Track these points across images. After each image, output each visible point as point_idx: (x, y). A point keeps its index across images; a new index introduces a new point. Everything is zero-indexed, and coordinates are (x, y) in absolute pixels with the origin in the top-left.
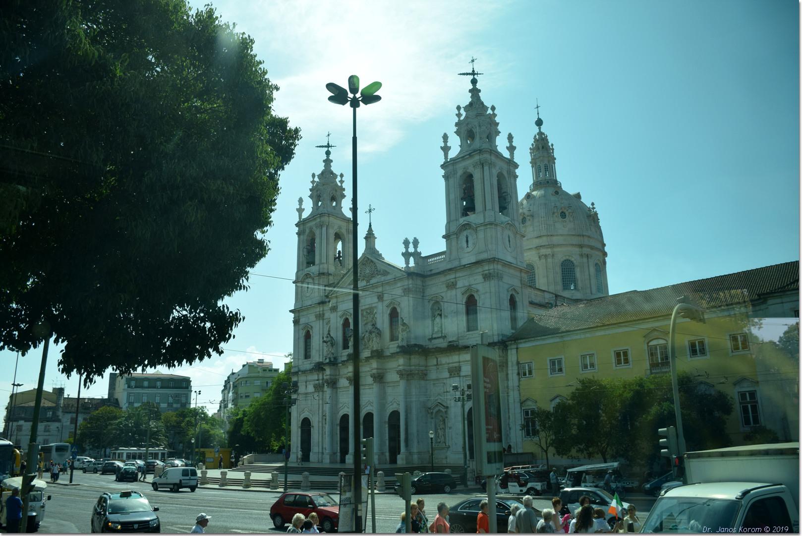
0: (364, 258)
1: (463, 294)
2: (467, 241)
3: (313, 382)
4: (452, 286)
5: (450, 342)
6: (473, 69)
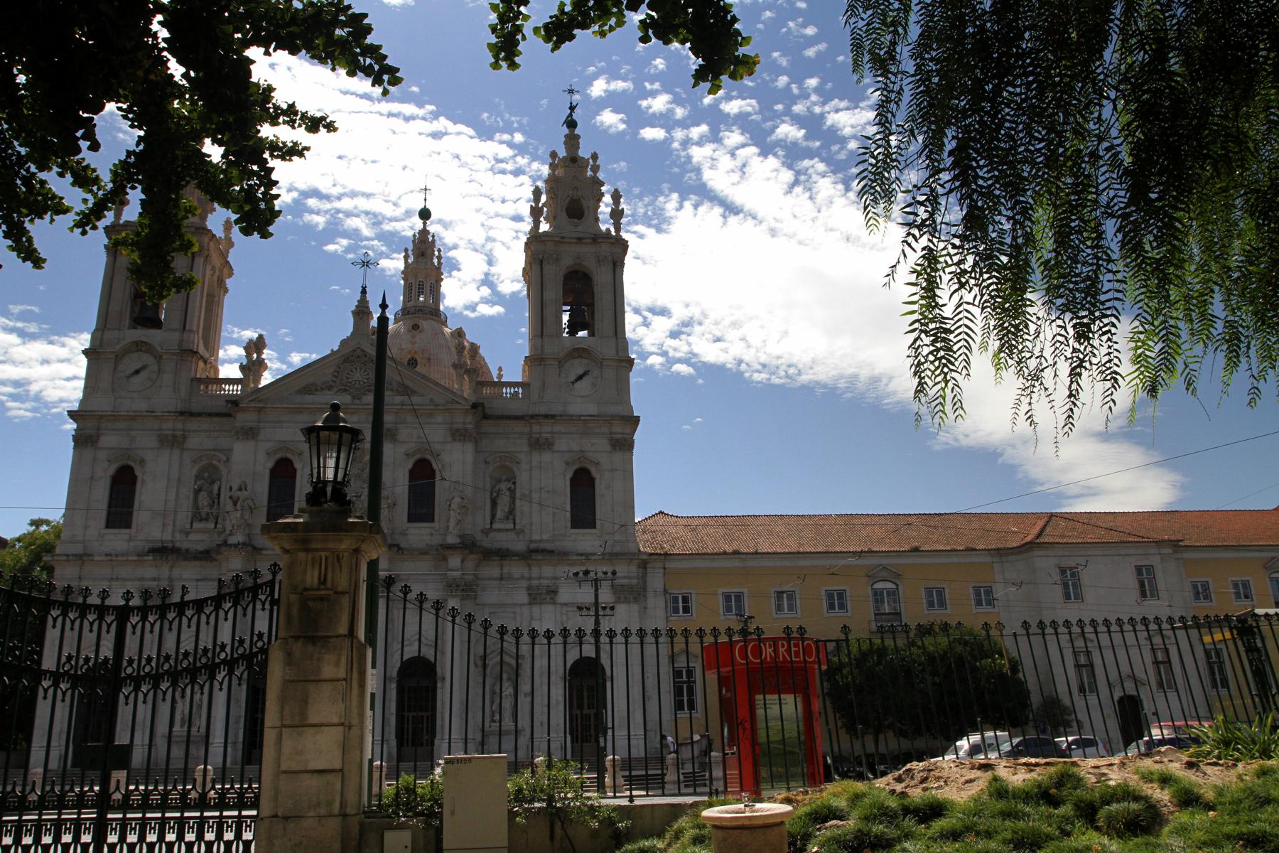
0: (354, 351)
1: (567, 464)
3: (139, 583)
4: (539, 444)
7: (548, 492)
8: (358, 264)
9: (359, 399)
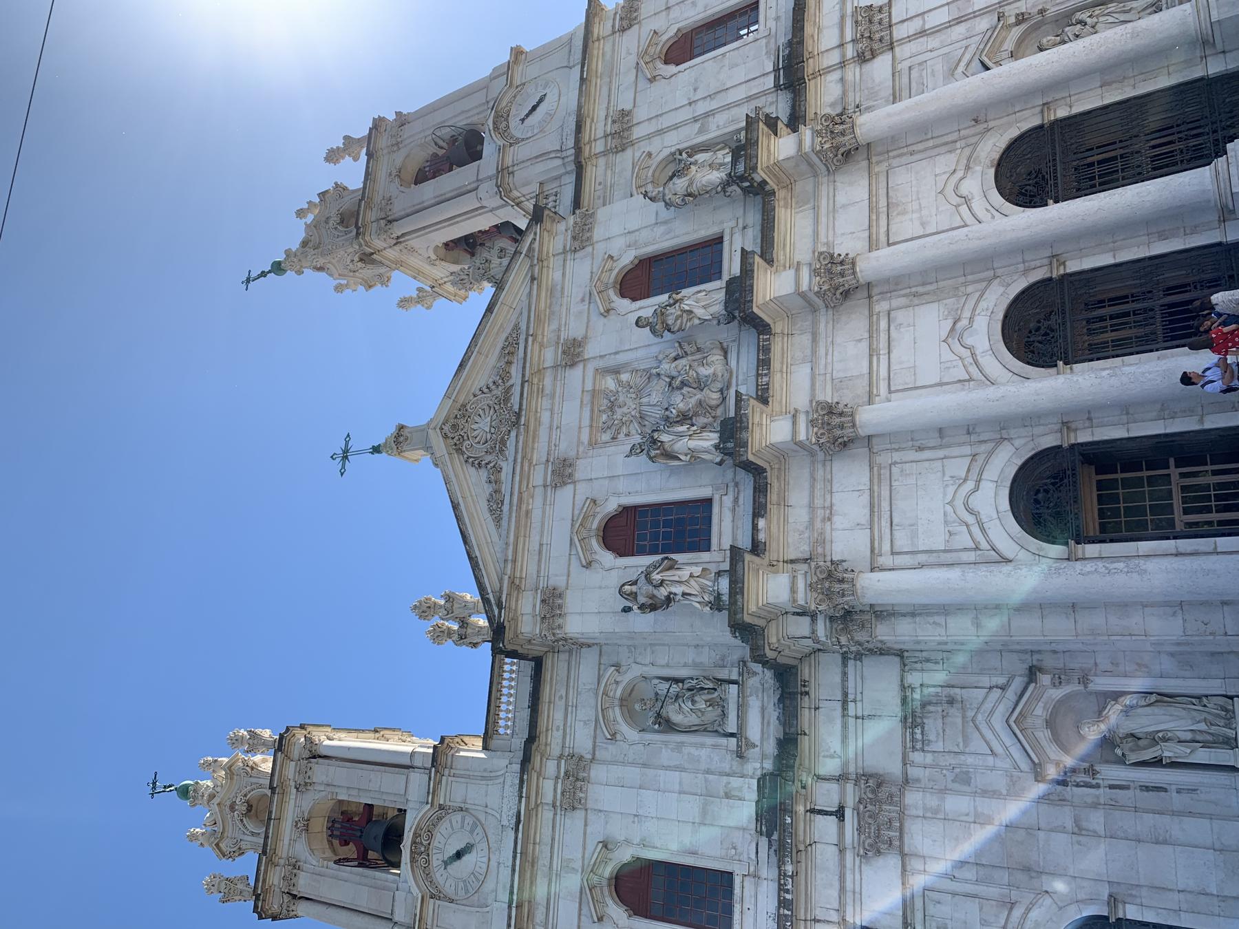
0: (445, 437)
2: (534, 108)
3: (849, 856)
5: (777, 86)
7: (695, 90)
8: (343, 467)
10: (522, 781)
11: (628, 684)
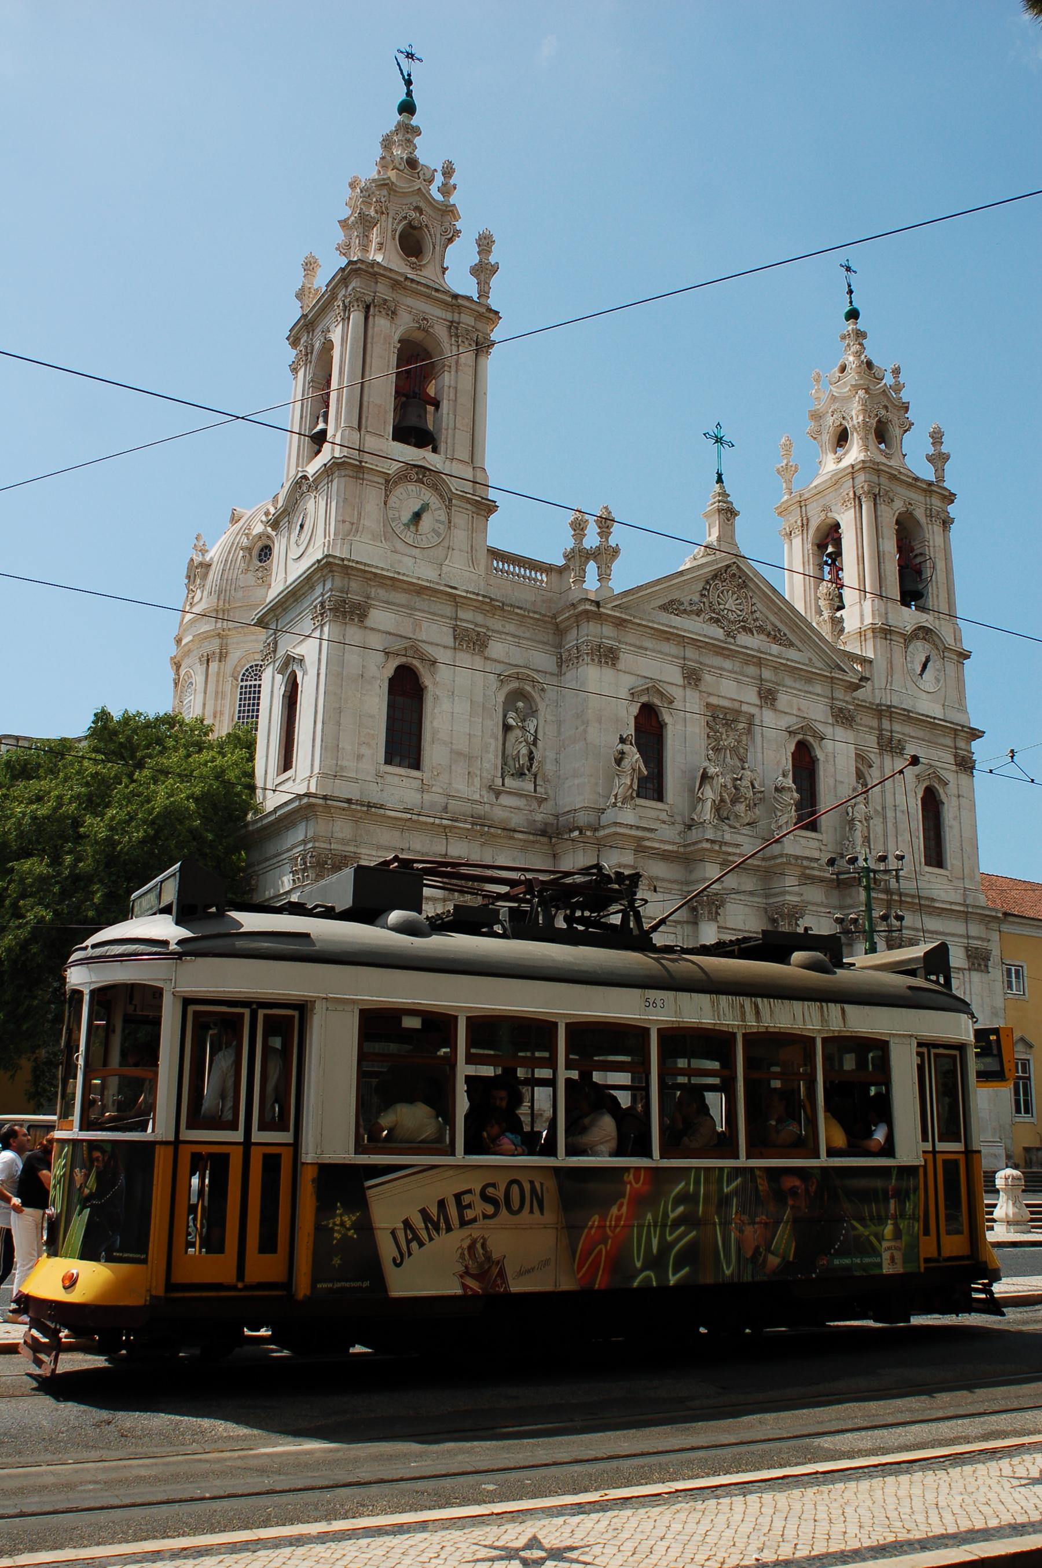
0: (728, 566)
2: (924, 667)
6: (849, 286)
8: (711, 437)
9: (734, 638)
10: (478, 594)
11: (532, 697)
